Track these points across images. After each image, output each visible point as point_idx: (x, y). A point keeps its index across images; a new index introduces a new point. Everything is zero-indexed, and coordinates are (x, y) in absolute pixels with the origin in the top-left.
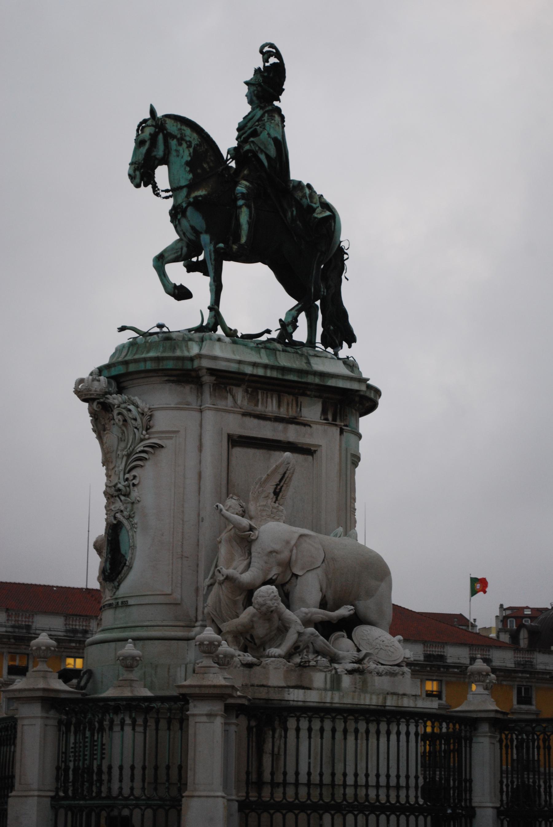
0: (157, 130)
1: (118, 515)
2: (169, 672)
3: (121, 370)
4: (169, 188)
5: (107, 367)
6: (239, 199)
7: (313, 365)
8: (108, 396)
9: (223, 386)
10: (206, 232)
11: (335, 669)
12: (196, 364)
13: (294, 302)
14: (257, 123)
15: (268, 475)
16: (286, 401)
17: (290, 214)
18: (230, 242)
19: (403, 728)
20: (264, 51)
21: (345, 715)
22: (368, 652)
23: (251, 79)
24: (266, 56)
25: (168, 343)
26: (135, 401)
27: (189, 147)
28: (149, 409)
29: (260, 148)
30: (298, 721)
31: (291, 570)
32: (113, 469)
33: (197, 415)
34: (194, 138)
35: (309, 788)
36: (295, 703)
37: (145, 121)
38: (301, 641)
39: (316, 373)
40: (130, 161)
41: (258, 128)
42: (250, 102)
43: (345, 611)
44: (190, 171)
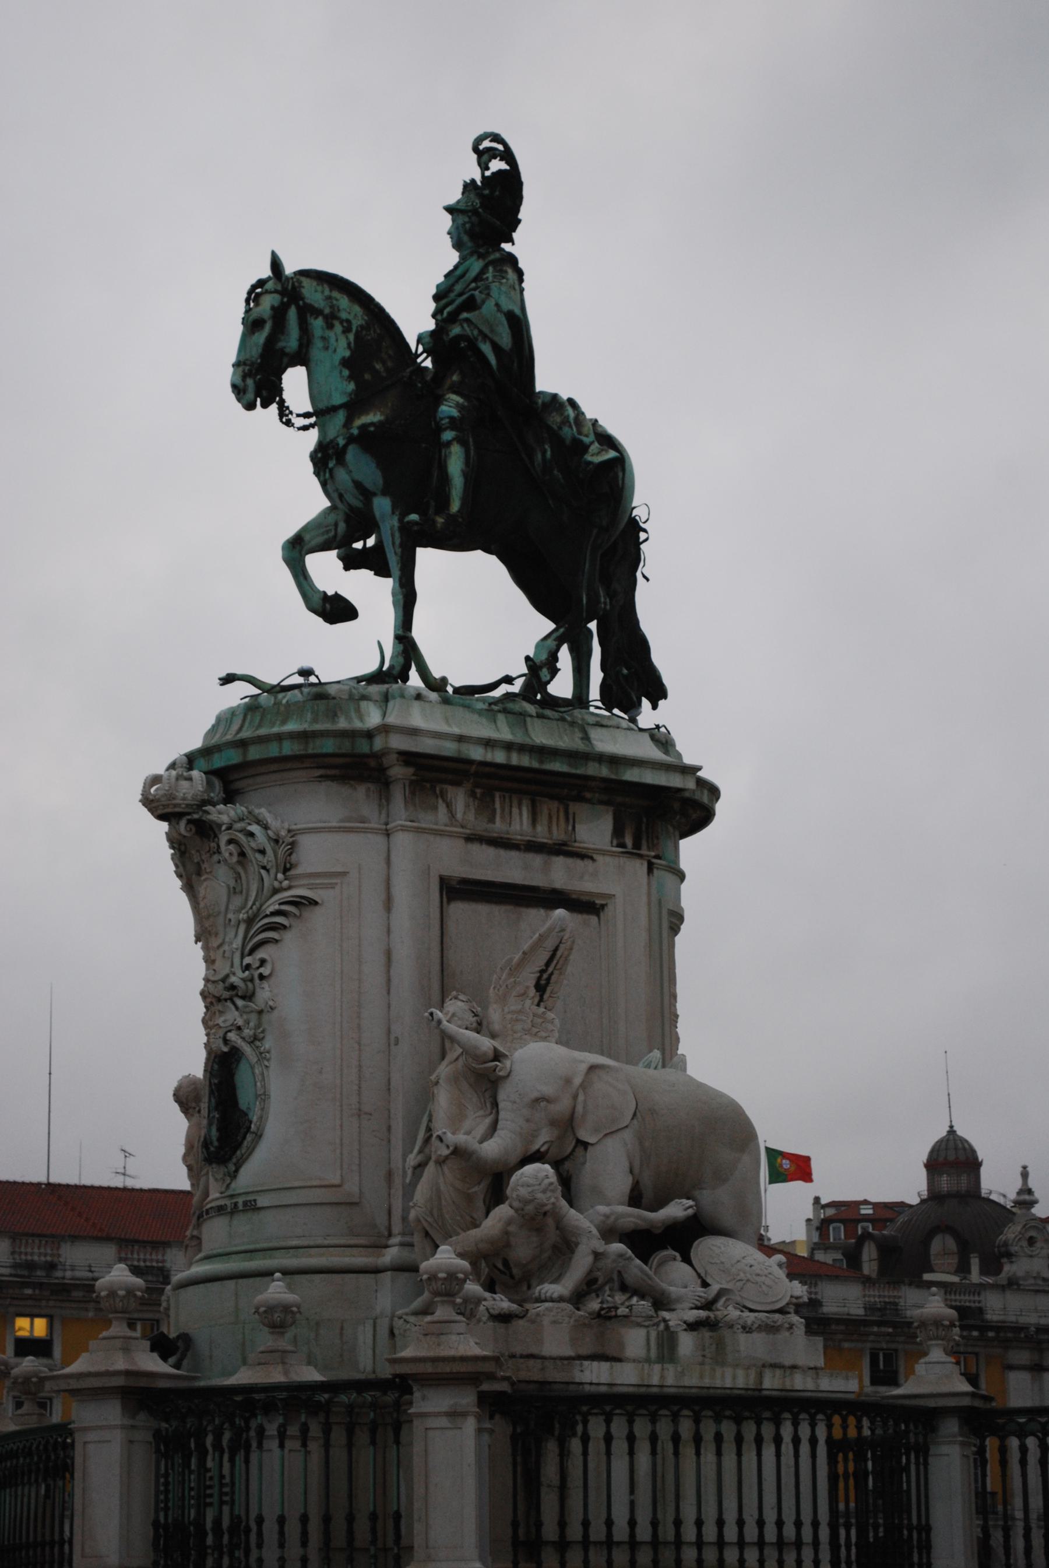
0: (285, 300)
1: (232, 1036)
2: (341, 1334)
3: (233, 757)
4: (311, 410)
5: (206, 752)
6: (445, 429)
7: (594, 742)
8: (209, 808)
9: (428, 785)
10: (384, 493)
11: (665, 1321)
12: (378, 744)
13: (548, 626)
14: (473, 285)
15: (524, 953)
16: (546, 812)
17: (539, 456)
18: (431, 511)
19: (805, 1431)
20: (481, 147)
21: (697, 1408)
22: (724, 1286)
23: (458, 202)
24: (483, 156)
25: (322, 705)
26: (261, 817)
27: (347, 330)
28: (289, 831)
29: (481, 332)
30: (631, 1422)
31: (574, 1134)
32: (219, 947)
33: (380, 840)
35: (586, 1551)
36: (593, 1389)
37: (261, 283)
38: (599, 1270)
39: (602, 758)
40: (233, 359)
41: (477, 293)
42: (458, 245)
43: (677, 1210)
44: (351, 378)
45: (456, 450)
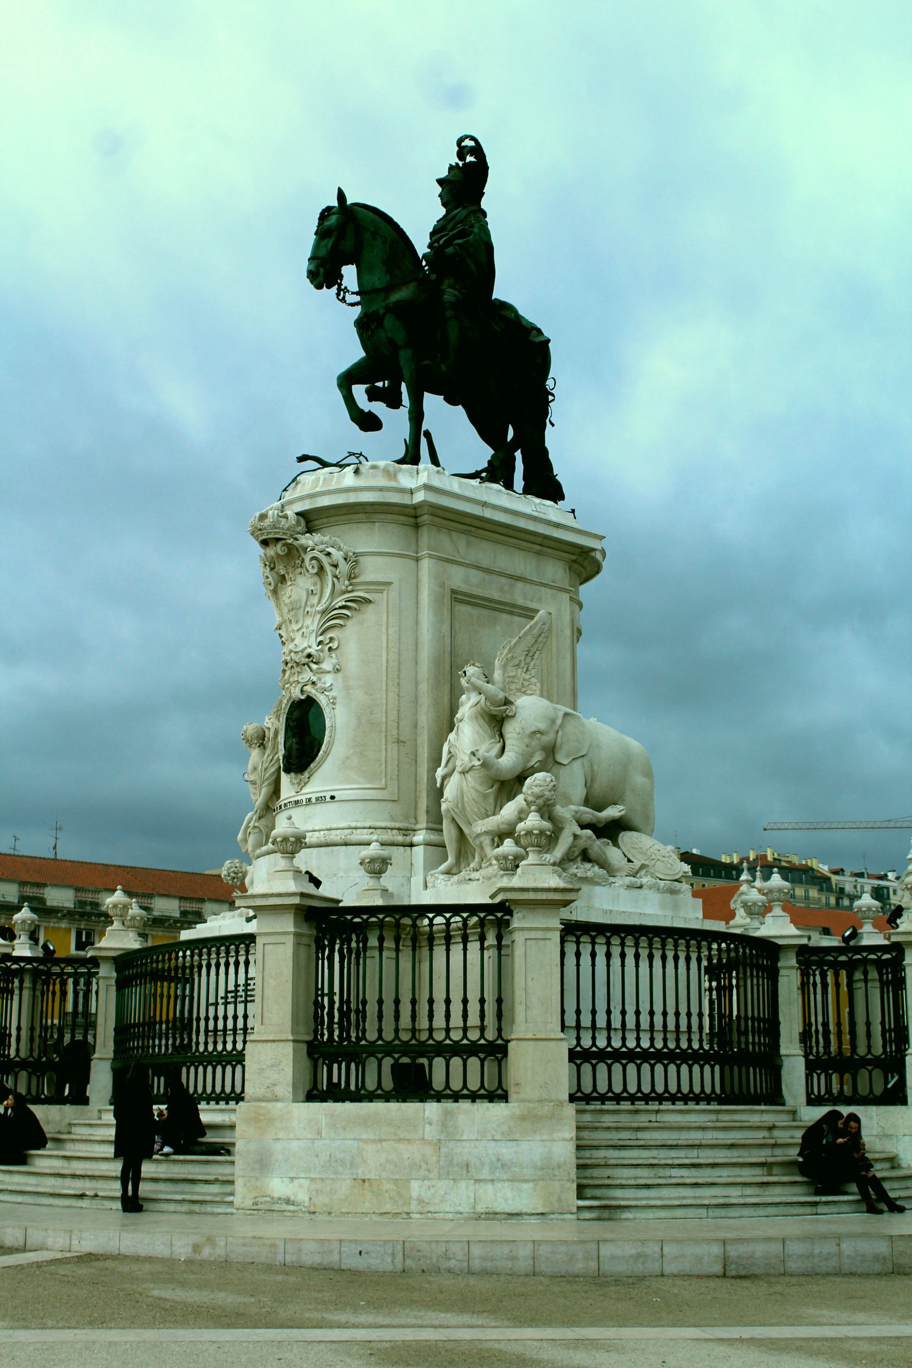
1: (308, 688)
20: (463, 144)
22: (643, 862)
27: (385, 242)
31: (554, 758)
32: (298, 630)
33: (412, 563)
37: (329, 209)
38: (575, 846)
40: (309, 256)
43: (612, 812)
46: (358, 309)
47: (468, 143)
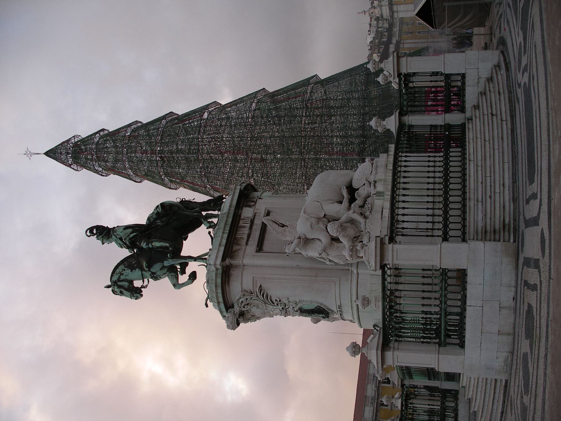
3: (222, 306)
5: (221, 312)
10: (163, 263)
12: (219, 267)
27: (124, 270)
34: (122, 267)
37: (112, 291)
39: (229, 209)
43: (345, 192)
45: (153, 244)
46: (150, 280)
47: (88, 234)
